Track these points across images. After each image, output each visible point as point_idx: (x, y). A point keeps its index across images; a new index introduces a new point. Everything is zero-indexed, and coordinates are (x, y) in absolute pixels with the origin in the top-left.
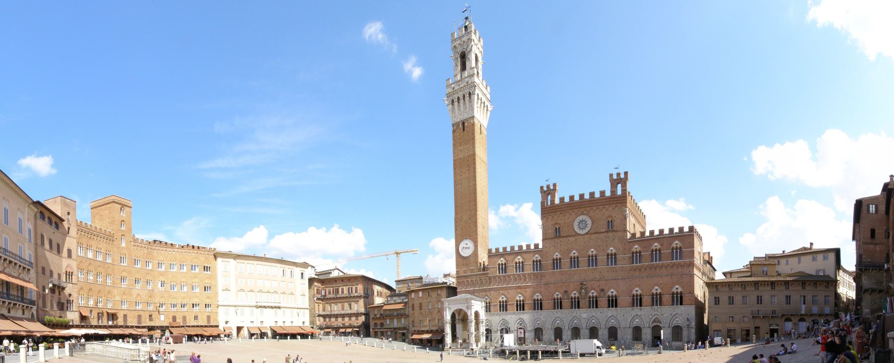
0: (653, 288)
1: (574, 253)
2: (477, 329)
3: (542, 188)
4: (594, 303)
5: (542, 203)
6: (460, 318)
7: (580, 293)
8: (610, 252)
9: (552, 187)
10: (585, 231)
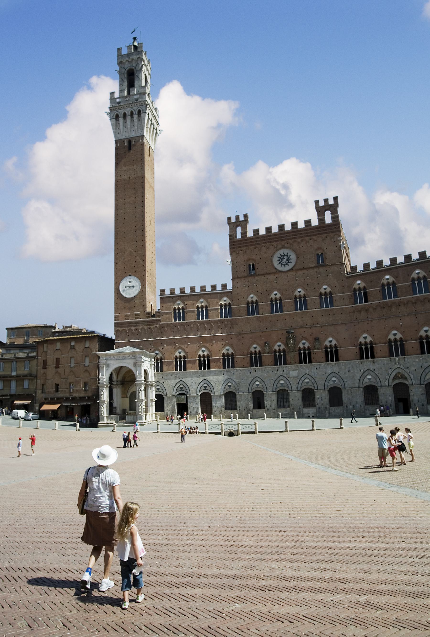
0: (389, 333)
1: (275, 294)
3: (229, 219)
4: (305, 357)
5: (232, 237)
6: (125, 380)
7: (287, 344)
8: (323, 291)
9: (242, 218)
10: (287, 268)
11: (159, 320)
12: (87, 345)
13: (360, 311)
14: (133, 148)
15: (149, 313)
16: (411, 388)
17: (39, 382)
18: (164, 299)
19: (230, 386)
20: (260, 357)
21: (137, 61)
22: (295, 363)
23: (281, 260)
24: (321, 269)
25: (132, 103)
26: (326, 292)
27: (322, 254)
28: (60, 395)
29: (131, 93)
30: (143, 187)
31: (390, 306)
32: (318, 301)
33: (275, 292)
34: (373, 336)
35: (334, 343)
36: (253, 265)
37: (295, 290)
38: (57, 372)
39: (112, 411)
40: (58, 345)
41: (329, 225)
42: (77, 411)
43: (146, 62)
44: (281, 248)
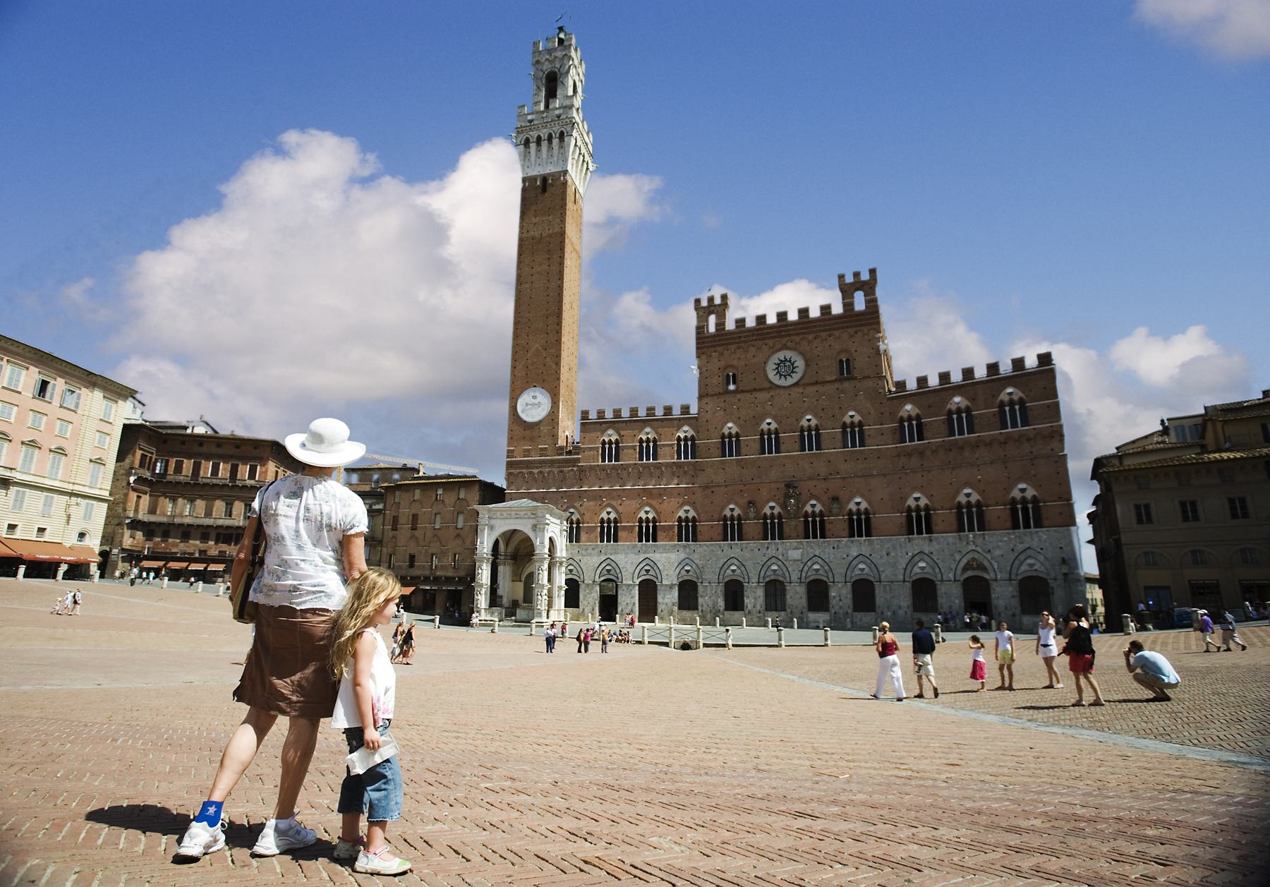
0: (958, 492)
1: (769, 423)
4: (815, 528)
5: (701, 330)
6: (516, 552)
7: (784, 506)
8: (847, 420)
9: (718, 301)
10: (790, 381)
11: (578, 460)
12: (462, 496)
13: (910, 455)
14: (550, 189)
15: (561, 448)
16: (994, 585)
17: (384, 550)
18: (587, 425)
19: (688, 571)
20: (740, 525)
22: (798, 537)
23: (782, 368)
24: (846, 385)
26: (852, 423)
27: (848, 360)
28: (415, 572)
30: (562, 249)
31: (960, 447)
32: (839, 437)
33: (769, 420)
34: (930, 497)
35: (864, 505)
36: (734, 375)
37: (802, 417)
38: (413, 536)
39: (494, 601)
40: (418, 492)
41: (861, 313)
42: (440, 600)
43: (576, 62)
44: (780, 350)
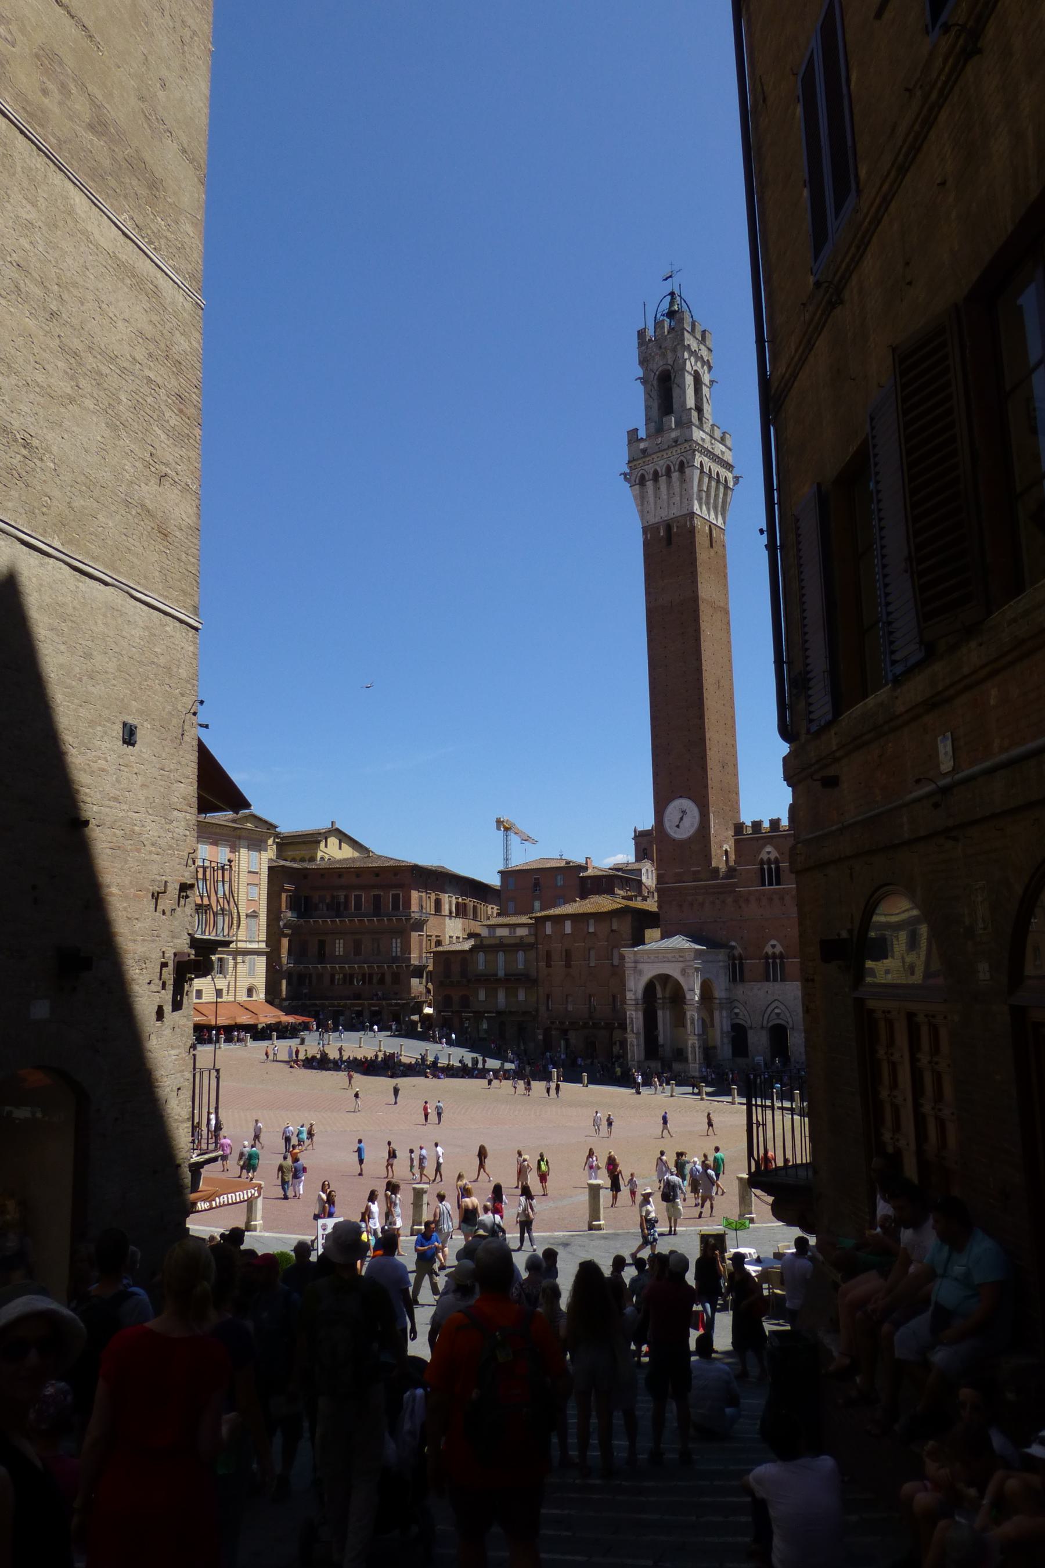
2: (706, 1025)
11: (735, 885)
12: (615, 927)
15: (717, 870)
21: (674, 350)
25: (669, 447)
29: (665, 428)
